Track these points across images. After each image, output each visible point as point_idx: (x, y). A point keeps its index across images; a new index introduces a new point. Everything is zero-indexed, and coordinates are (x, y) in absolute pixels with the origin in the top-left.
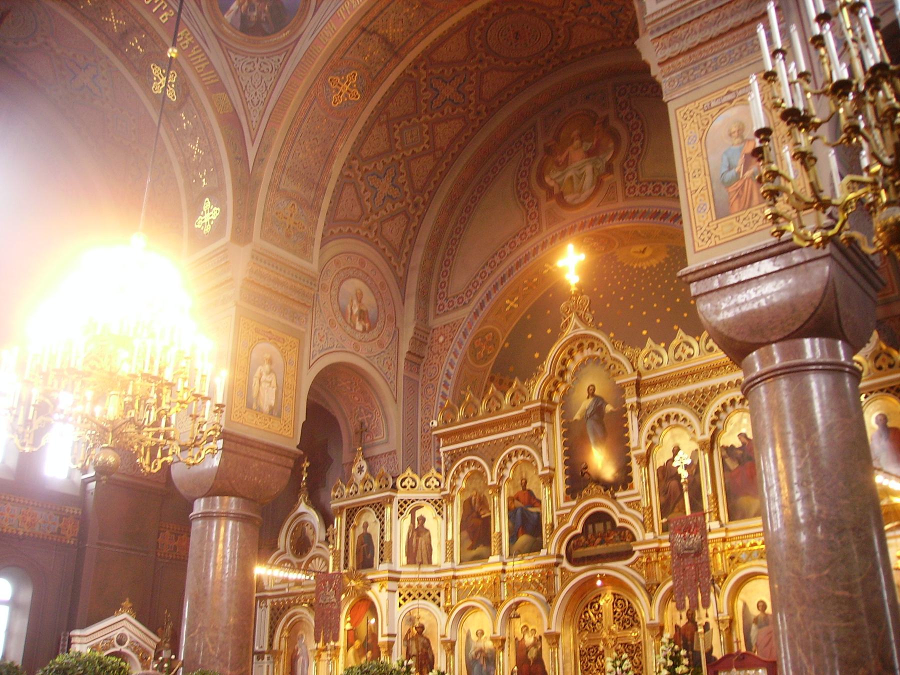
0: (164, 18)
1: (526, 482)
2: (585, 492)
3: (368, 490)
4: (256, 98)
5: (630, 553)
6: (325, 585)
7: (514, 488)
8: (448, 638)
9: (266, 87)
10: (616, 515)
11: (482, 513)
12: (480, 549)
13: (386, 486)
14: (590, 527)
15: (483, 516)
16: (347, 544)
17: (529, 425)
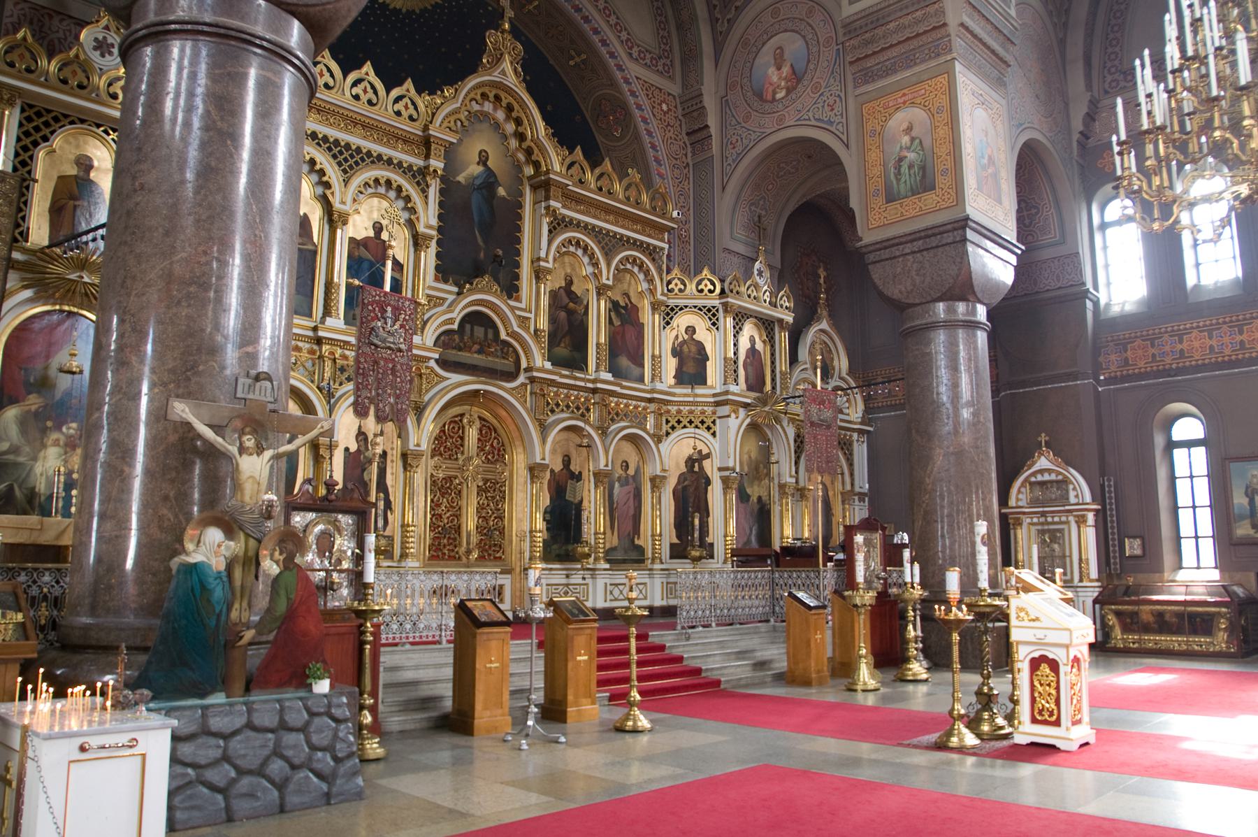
5: (512, 376)
6: (384, 311)
14: (468, 327)
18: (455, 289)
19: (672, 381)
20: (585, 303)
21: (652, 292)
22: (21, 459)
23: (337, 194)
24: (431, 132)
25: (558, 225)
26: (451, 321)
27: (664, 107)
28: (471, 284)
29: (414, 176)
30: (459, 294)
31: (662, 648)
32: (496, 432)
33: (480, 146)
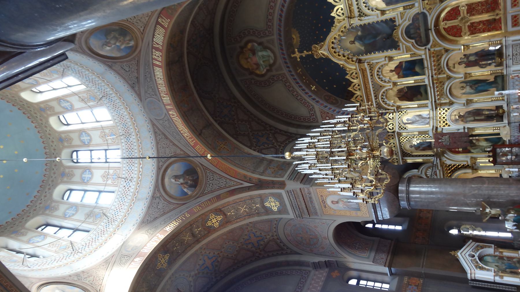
0: (188, 215)
1: (391, 70)
2: (396, 40)
3: (394, 145)
4: (224, 183)
6: (440, 142)
7: (393, 75)
8: (465, 102)
9: (220, 178)
10: (407, 23)
11: (405, 91)
12: (422, 90)
13: (392, 136)
14: (412, 36)
15: (407, 90)
16: (420, 156)
17: (365, 69)
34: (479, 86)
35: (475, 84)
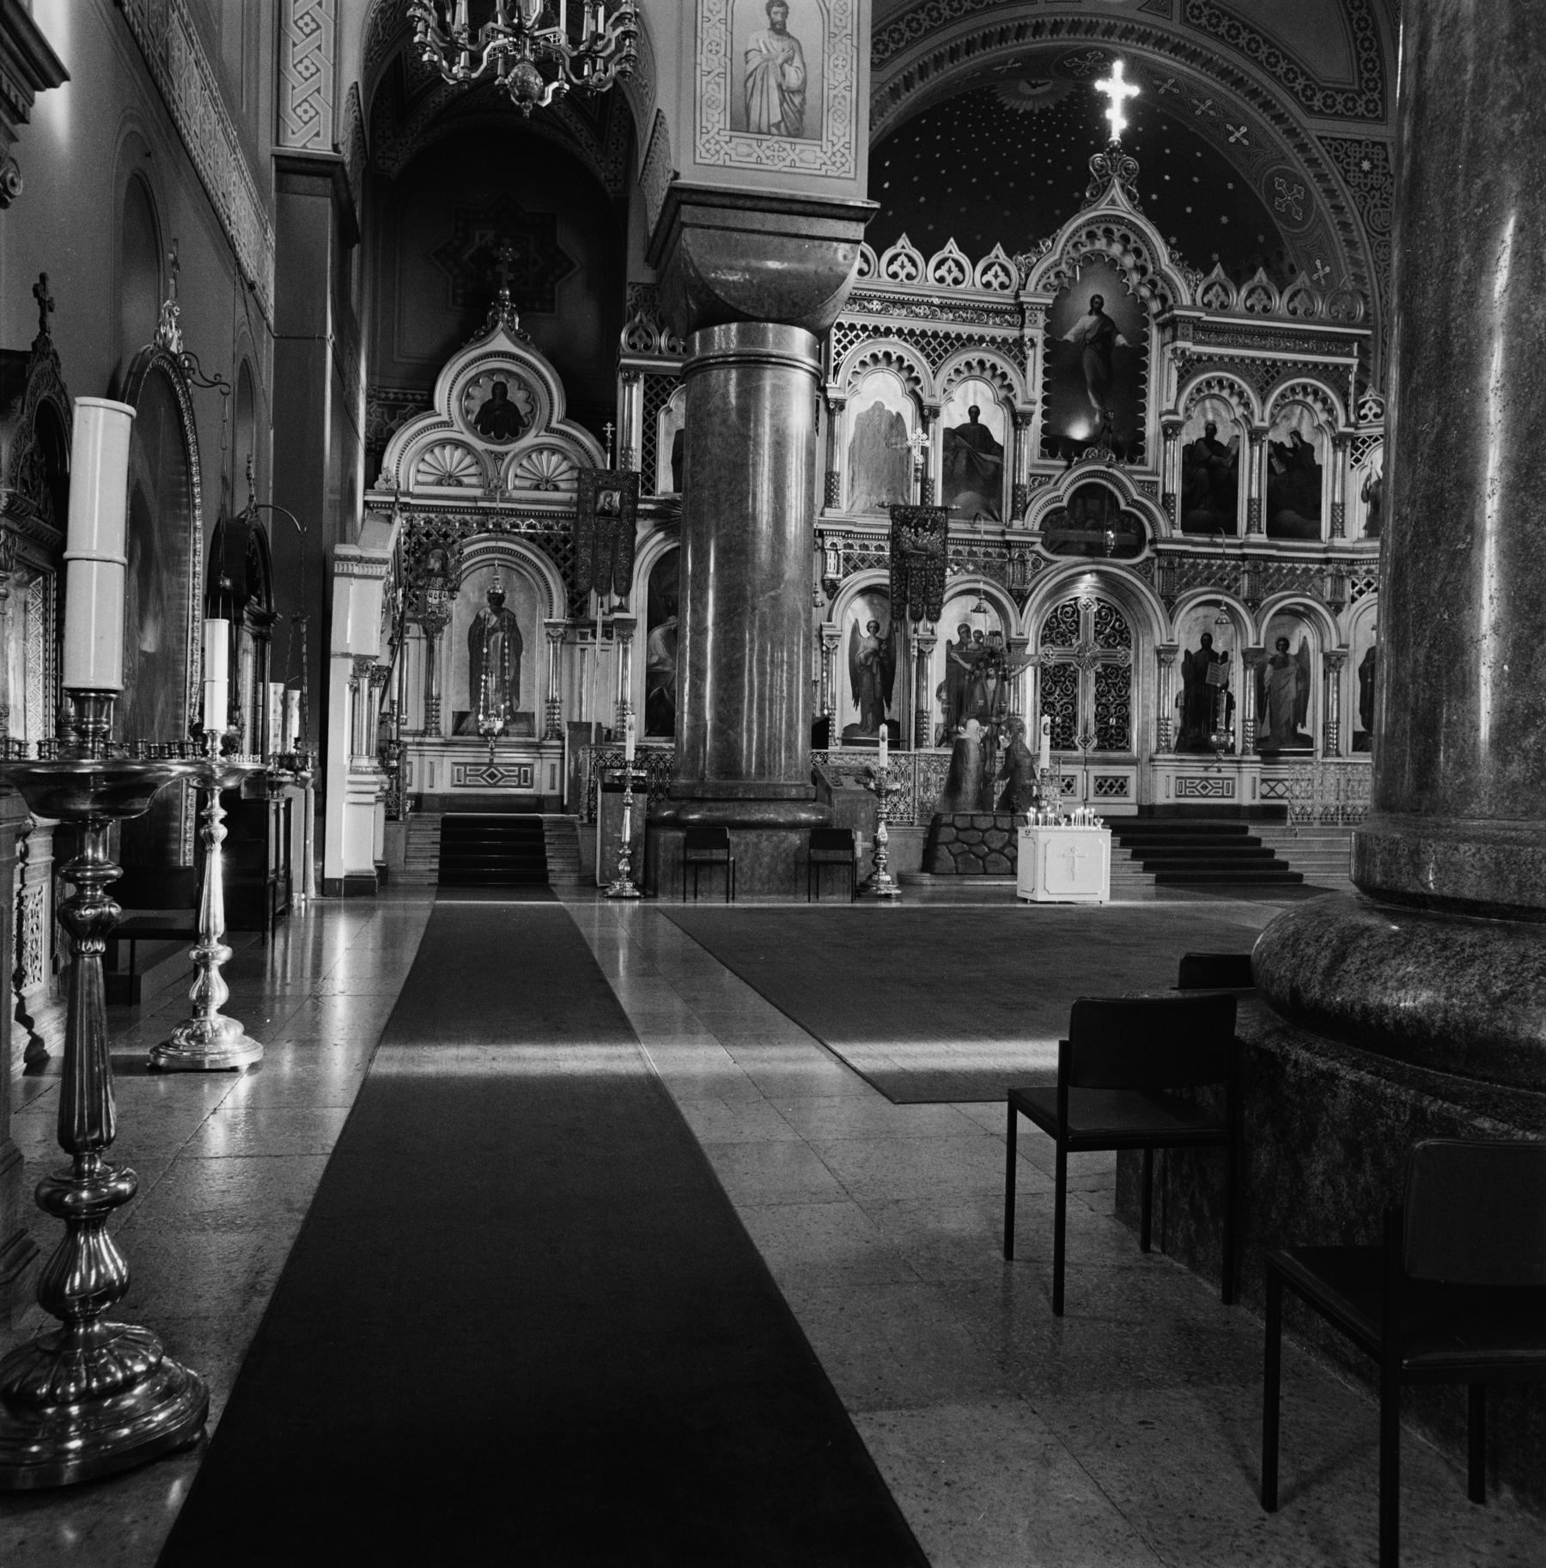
14: (1080, 501)
18: (1064, 463)
19: (1362, 533)
20: (1234, 452)
21: (1332, 424)
22: (667, 669)
23: (926, 389)
24: (1022, 299)
25: (1189, 367)
26: (1059, 499)
27: (1366, 165)
28: (1080, 455)
29: (1010, 351)
30: (1068, 468)
31: (1258, 841)
32: (1118, 613)
33: (1091, 291)
34: (874, 676)
35: (881, 665)
